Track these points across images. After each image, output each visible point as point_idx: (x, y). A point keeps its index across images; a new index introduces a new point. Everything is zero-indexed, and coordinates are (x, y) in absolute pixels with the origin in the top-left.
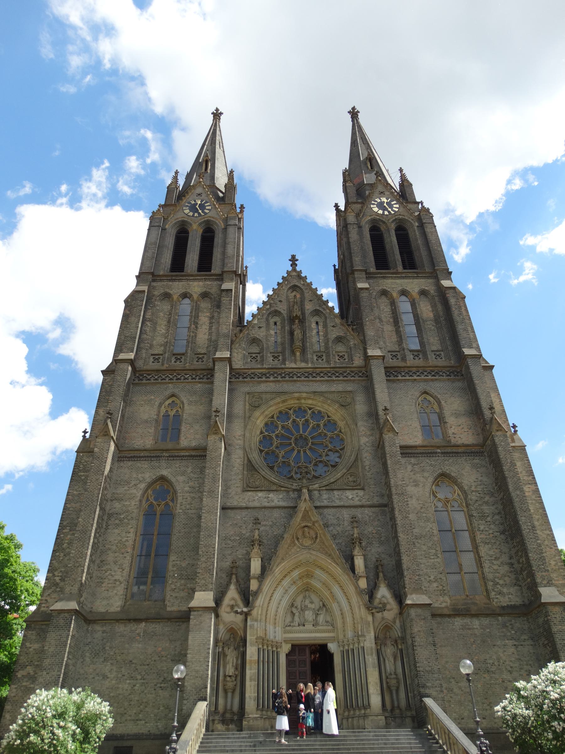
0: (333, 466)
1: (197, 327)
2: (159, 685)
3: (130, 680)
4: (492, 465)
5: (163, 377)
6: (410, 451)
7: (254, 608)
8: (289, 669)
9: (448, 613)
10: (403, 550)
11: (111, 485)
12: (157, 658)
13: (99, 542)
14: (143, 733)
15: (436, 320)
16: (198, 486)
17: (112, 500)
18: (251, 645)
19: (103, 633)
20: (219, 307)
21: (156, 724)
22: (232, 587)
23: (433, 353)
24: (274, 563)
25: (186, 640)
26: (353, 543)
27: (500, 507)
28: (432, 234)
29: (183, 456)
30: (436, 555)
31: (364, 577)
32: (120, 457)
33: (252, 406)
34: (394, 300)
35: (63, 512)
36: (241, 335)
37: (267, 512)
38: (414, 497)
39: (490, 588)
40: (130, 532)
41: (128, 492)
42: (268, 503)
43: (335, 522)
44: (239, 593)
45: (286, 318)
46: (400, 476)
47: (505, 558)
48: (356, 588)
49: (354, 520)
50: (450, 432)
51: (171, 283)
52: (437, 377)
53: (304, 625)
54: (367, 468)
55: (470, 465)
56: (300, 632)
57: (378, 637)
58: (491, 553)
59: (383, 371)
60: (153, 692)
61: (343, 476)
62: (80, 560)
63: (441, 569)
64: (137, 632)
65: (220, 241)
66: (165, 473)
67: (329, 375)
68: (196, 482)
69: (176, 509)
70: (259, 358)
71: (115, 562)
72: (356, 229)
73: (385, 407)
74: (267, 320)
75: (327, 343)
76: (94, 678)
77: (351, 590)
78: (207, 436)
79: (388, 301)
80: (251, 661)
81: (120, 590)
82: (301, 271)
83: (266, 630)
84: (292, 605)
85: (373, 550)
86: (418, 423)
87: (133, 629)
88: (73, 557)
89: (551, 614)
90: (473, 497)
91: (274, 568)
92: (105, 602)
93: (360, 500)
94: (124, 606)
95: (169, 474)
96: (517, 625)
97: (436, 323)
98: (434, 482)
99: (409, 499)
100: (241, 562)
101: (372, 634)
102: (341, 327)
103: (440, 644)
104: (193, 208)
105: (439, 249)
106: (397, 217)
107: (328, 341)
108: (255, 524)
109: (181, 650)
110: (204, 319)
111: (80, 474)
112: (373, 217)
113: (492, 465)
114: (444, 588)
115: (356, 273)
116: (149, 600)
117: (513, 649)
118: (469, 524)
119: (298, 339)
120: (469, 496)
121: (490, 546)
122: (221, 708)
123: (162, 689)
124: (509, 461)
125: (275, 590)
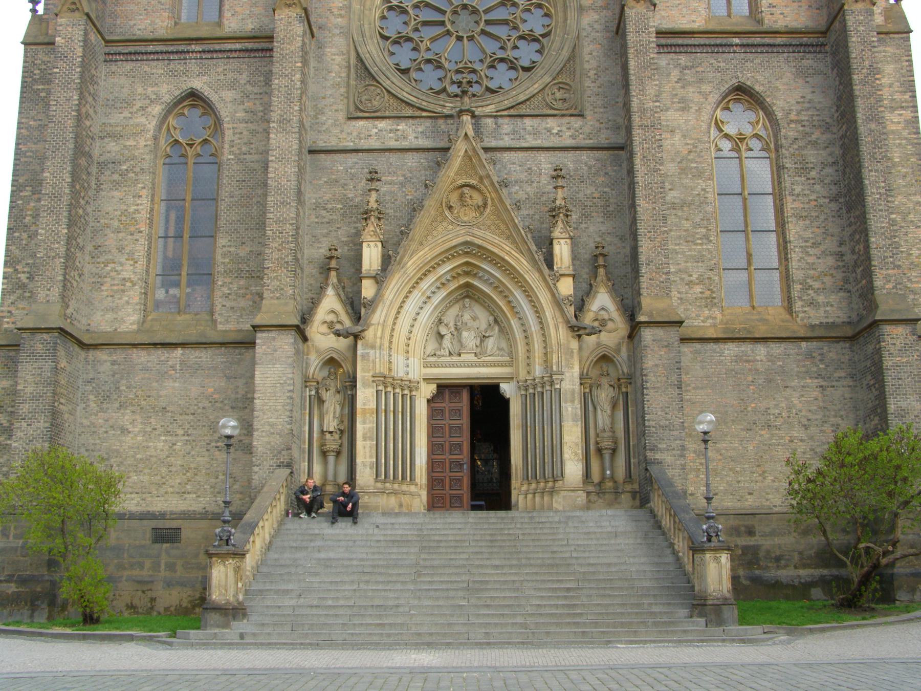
0: (526, 69)
2: (213, 444)
3: (165, 435)
6: (680, 41)
9: (715, 336)
10: (642, 229)
11: (98, 109)
12: (208, 405)
13: (88, 214)
14: (194, 511)
16: (261, 109)
17: (102, 138)
18: (365, 385)
21: (214, 499)
22: (330, 291)
24: (405, 251)
26: (554, 216)
27: (838, 151)
29: (231, 51)
30: (706, 237)
32: (109, 54)
35: (15, 159)
37: (394, 158)
39: (795, 294)
41: (131, 122)
42: (397, 140)
43: (523, 176)
46: (651, 91)
47: (830, 244)
48: (553, 295)
49: (558, 174)
53: (460, 355)
55: (794, 69)
56: (453, 365)
57: (587, 374)
58: (808, 234)
60: (207, 453)
61: (543, 89)
62: (56, 246)
66: (197, 84)
68: (257, 102)
69: (222, 154)
71: (120, 250)
76: (106, 432)
77: (544, 298)
78: (274, 10)
80: (364, 411)
81: (135, 295)
84: (440, 322)
85: (592, 229)
87: (163, 358)
88: (44, 241)
90: (789, 132)
91: (405, 259)
92: (109, 316)
94: (144, 322)
96: (831, 354)
98: (720, 102)
99: (668, 135)
101: (576, 370)
108: (372, 180)
109: (246, 392)
111: (35, 87)
113: (835, 70)
114: (714, 295)
116: (185, 313)
117: (816, 393)
118: (776, 183)
120: (783, 131)
121: (808, 222)
123: (220, 450)
124: (867, 63)
125: (407, 297)
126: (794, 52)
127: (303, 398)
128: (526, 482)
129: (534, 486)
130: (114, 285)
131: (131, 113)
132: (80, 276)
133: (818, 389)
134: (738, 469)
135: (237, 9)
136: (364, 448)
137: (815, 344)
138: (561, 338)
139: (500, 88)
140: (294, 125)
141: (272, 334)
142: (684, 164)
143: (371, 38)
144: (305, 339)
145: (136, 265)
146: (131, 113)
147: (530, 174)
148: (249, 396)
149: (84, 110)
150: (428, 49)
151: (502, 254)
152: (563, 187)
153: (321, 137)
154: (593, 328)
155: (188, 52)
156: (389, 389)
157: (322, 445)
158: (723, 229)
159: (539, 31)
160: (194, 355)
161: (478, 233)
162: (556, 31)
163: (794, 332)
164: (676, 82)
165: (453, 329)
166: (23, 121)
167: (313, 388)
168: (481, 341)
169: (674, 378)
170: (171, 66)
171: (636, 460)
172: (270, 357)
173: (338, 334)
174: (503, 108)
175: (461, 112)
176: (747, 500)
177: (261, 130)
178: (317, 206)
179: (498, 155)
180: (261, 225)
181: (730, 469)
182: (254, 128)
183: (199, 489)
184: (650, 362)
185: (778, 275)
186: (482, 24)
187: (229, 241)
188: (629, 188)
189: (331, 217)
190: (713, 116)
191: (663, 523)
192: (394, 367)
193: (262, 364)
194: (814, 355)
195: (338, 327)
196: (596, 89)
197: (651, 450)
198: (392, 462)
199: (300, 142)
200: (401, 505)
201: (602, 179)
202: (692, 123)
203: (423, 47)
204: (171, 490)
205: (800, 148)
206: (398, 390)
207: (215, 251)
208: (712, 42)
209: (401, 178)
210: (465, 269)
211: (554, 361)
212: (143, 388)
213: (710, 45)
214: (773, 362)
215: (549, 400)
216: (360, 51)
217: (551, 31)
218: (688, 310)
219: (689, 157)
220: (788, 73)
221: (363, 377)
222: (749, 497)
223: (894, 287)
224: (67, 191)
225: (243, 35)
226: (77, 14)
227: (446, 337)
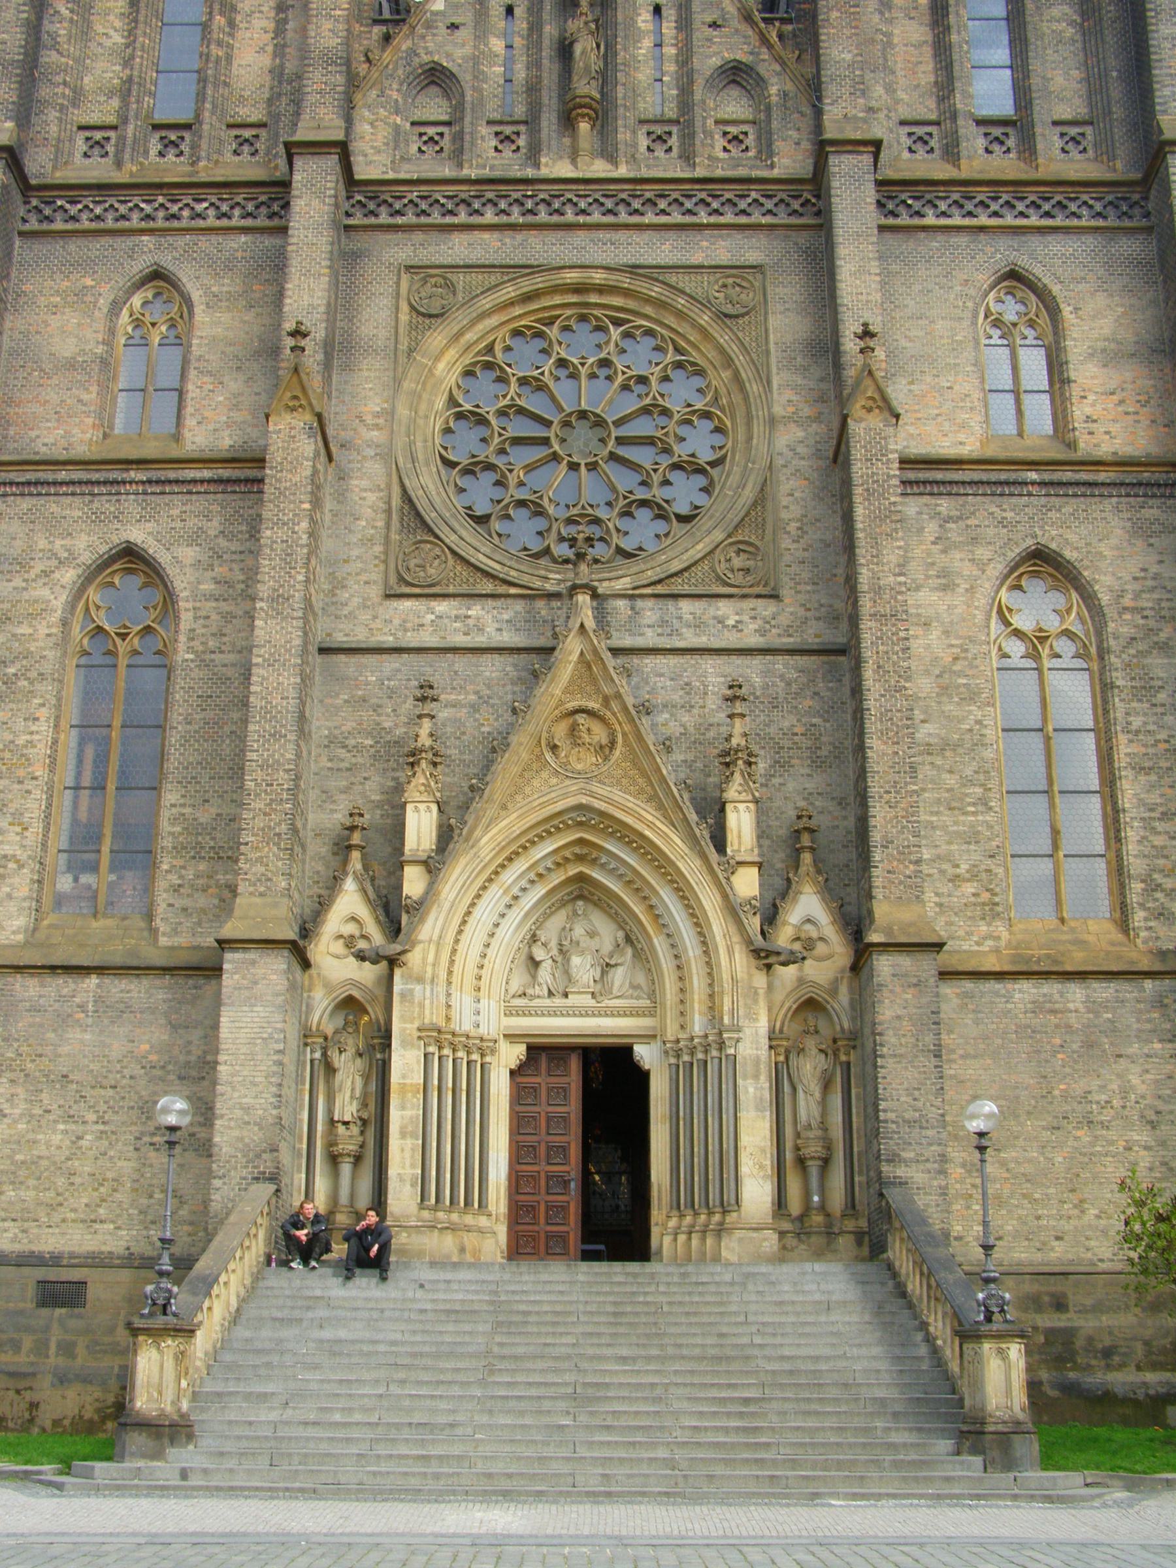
0: (683, 519)
2: (147, 1139)
3: (65, 1122)
5: (123, 209)
6: (939, 476)
7: (413, 946)
8: (518, 1108)
9: (997, 969)
10: (875, 786)
16: (242, 577)
18: (405, 1044)
22: (350, 885)
24: (478, 819)
25: (216, 1026)
26: (727, 765)
29: (194, 481)
31: (752, 864)
33: (419, 313)
36: (387, 56)
37: (460, 663)
40: (37, 719)
43: (677, 697)
46: (891, 557)
48: (725, 896)
49: (734, 694)
50: (1079, 412)
52: (1058, 221)
53: (566, 995)
55: (1129, 524)
58: (1154, 798)
59: (870, 194)
60: (135, 1155)
61: (712, 552)
63: (994, 843)
64: (77, 1000)
66: (137, 535)
67: (688, 204)
68: (234, 566)
70: (446, 143)
73: (865, 325)
77: (710, 900)
78: (267, 416)
80: (403, 1087)
83: (449, 1006)
84: (534, 939)
85: (791, 786)
86: (977, 382)
87: (65, 991)
91: (478, 833)
93: (762, 632)
94: (35, 929)
98: (1007, 577)
99: (920, 631)
101: (763, 1024)
103: (961, 1052)
107: (691, 82)
108: (423, 699)
109: (205, 1052)
114: (997, 899)
116: (105, 916)
118: (1100, 711)
119: (587, 69)
120: (1111, 626)
121: (1153, 778)
125: (478, 896)
126: (1128, 495)
127: (300, 1063)
128: (675, 1213)
129: (688, 1219)
134: (1037, 1196)
135: (206, 414)
139: (640, 549)
140: (296, 606)
141: (252, 955)
143: (428, 465)
144: (306, 964)
145: (27, 834)
148: (209, 1058)
150: (521, 484)
151: (639, 826)
152: (743, 716)
153: (341, 626)
154: (792, 952)
155: (124, 482)
156: (446, 1051)
157: (331, 1144)
158: (1012, 788)
159: (705, 456)
160: (119, 988)
161: (600, 791)
163: (1132, 962)
164: (933, 543)
165: (555, 952)
167: (318, 1047)
169: (929, 1039)
171: (864, 1179)
172: (247, 993)
173: (361, 957)
174: (645, 582)
176: (1052, 1249)
178: (331, 741)
179: (636, 660)
180: (237, 771)
181: (1024, 1196)
182: (228, 609)
183: (118, 1216)
185: (1104, 866)
186: (611, 443)
187: (183, 796)
188: (855, 719)
189: (354, 760)
190: (994, 600)
191: (910, 1287)
193: (232, 1004)
194: (1166, 1001)
195: (362, 945)
196: (800, 554)
197: (888, 1161)
198: (448, 1176)
199: (306, 634)
200: (462, 1250)
201: (808, 702)
202: (959, 610)
203: (512, 480)
205: (1141, 654)
206: (460, 1054)
207: (157, 814)
208: (993, 477)
209: (473, 697)
210: (577, 850)
211: (726, 1008)
212: (31, 1041)
213: (988, 483)
214: (1097, 1014)
216: (407, 482)
218: (951, 924)
221: (405, 1029)
222: (1057, 1243)
227: (544, 964)
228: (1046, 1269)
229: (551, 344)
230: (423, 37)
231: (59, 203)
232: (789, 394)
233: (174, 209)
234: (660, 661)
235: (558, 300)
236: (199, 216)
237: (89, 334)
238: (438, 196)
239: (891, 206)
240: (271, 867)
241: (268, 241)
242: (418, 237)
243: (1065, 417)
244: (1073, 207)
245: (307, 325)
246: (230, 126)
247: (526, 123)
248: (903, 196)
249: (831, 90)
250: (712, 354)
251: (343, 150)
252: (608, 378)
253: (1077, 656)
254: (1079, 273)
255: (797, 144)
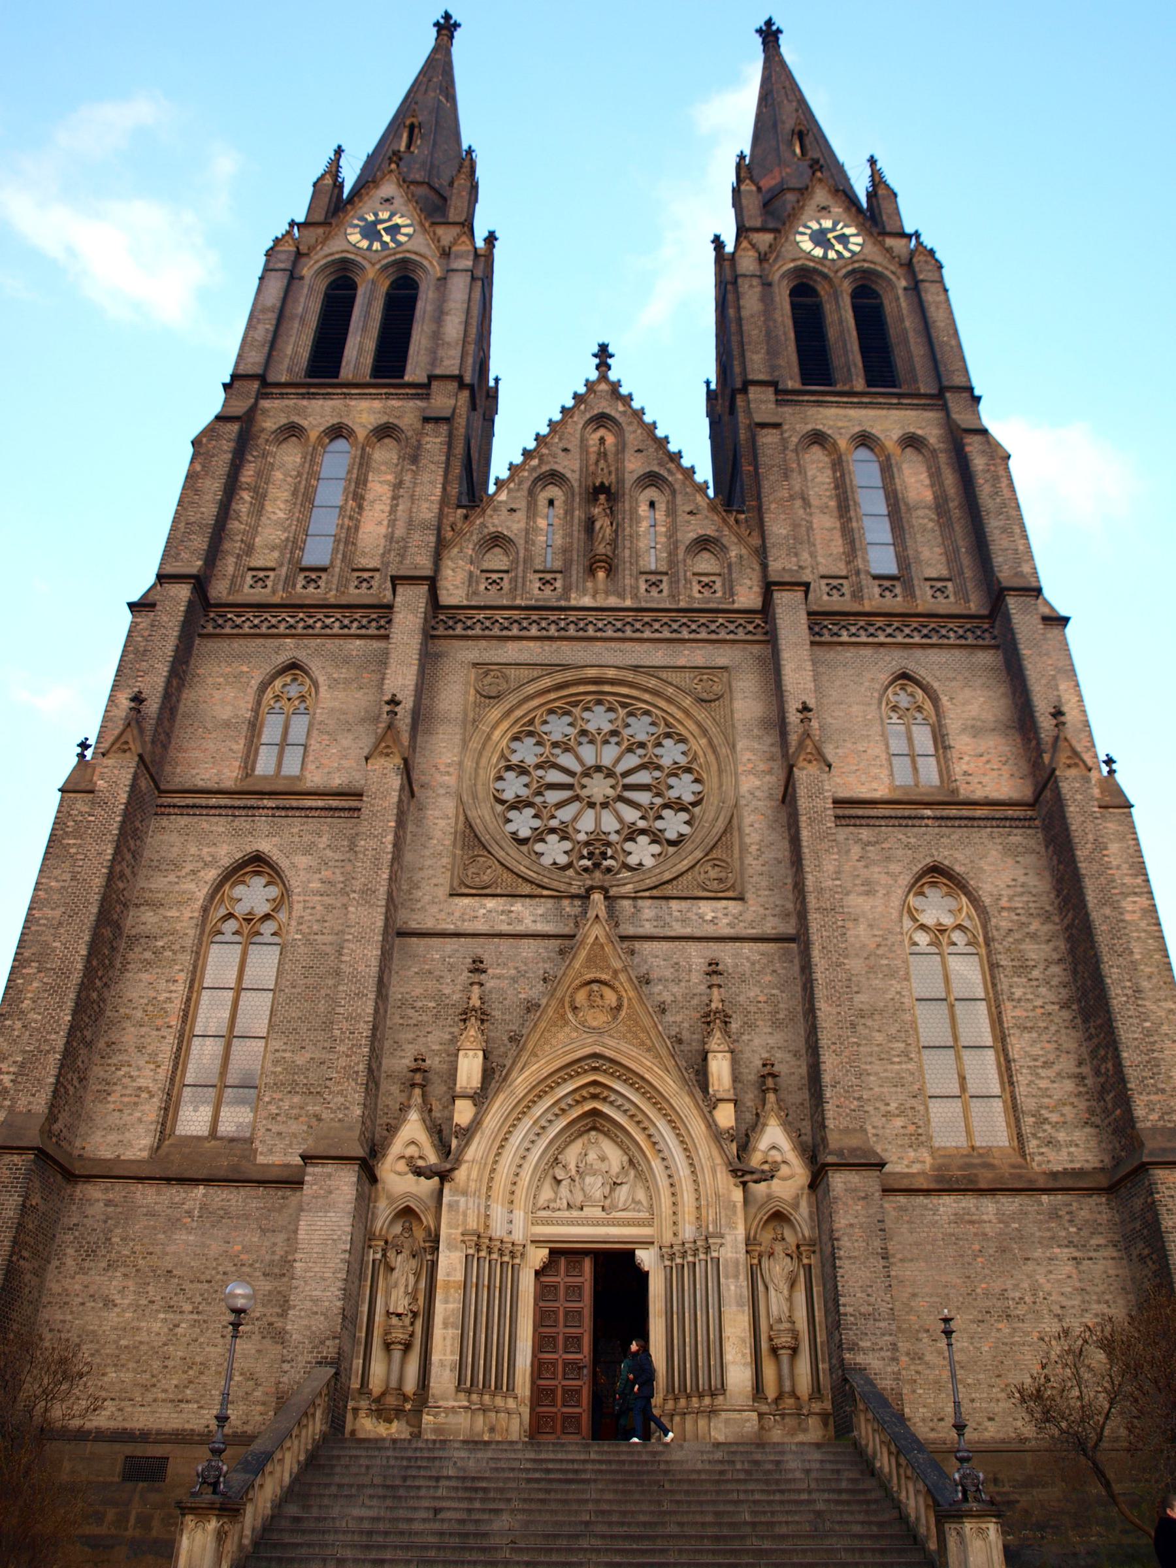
0: (671, 843)
1: (360, 507)
4: (1051, 848)
5: (274, 621)
6: (860, 812)
7: (460, 1165)
8: (541, 1304)
9: (925, 1186)
10: (825, 1039)
15: (940, 506)
16: (342, 879)
18: (451, 1247)
19: (106, 1205)
20: (415, 459)
22: (414, 1116)
23: (929, 583)
26: (708, 1023)
28: (938, 308)
29: (311, 809)
30: (905, 1054)
33: (481, 695)
34: (840, 457)
37: (504, 945)
38: (861, 920)
39: (1027, 1130)
41: (177, 888)
42: (509, 924)
43: (668, 973)
44: (428, 1129)
45: (577, 490)
46: (829, 866)
47: (1067, 1064)
48: (709, 1126)
49: (714, 969)
50: (958, 768)
51: (305, 402)
52: (934, 640)
54: (753, 848)
55: (1000, 847)
58: (1036, 1050)
62: (53, 1036)
63: (916, 1087)
65: (429, 308)
66: (265, 846)
67: (675, 626)
68: (337, 871)
71: (140, 1049)
72: (758, 289)
73: (804, 703)
74: (531, 492)
75: (672, 553)
77: (697, 1128)
79: (826, 459)
80: (447, 1283)
82: (619, 381)
85: (757, 1042)
88: (38, 1030)
89: (1162, 1188)
90: (1002, 921)
91: (514, 1074)
92: (113, 1138)
94: (158, 1148)
95: (275, 850)
96: (1082, 1213)
97: (938, 514)
98: (913, 885)
99: (849, 924)
100: (437, 1059)
101: (741, 1231)
102: (710, 515)
103: (899, 1256)
104: (370, 232)
105: (953, 342)
106: (856, 265)
107: (676, 548)
109: (286, 1252)
110: (379, 488)
111: (65, 841)
112: (799, 263)
114: (920, 1131)
115: (752, 389)
117: (1069, 1268)
120: (994, 921)
121: (1034, 1035)
122: (376, 1383)
126: (998, 827)
130: (125, 1095)
131: (178, 877)
132: (81, 1080)
133: (1070, 1263)
134: (970, 1381)
136: (444, 1339)
137: (1060, 1198)
138: (720, 1186)
140: (381, 897)
141: (329, 1169)
142: (872, 960)
144: (373, 1179)
145: (159, 1070)
146: (178, 877)
147: (677, 971)
148: (290, 1258)
149: (118, 868)
152: (720, 986)
154: (763, 1172)
155: (259, 808)
159: (688, 798)
160: (220, 1196)
161: (610, 1043)
162: (708, 799)
163: (1030, 1181)
165: (573, 1172)
166: (43, 881)
167: (379, 1249)
168: (612, 1190)
169: (877, 1243)
170: (235, 824)
171: (827, 1366)
172: (321, 1201)
173: (418, 1172)
175: (590, 890)
176: (986, 1429)
177: (339, 905)
178: (403, 1004)
179: (637, 945)
182: (330, 902)
183: (202, 1396)
184: (842, 1221)
185: (1001, 1104)
187: (285, 1044)
192: (493, 1224)
194: (1060, 1213)
195: (420, 1163)
196: (759, 868)
197: (850, 1350)
198: (482, 1362)
199: (387, 919)
200: (492, 1430)
201: (768, 978)
202: (879, 909)
204: (164, 1396)
208: (899, 813)
209: (513, 972)
210: (592, 1090)
212: (146, 1240)
213: (896, 818)
214: (1007, 1224)
215: (703, 1274)
216: (469, 813)
217: (702, 799)
219: (879, 952)
220: (994, 853)
221: (450, 1235)
222: (990, 1423)
223: (1161, 1118)
224: (80, 966)
225: (327, 790)
226: (128, 754)
228: (983, 1447)
229: (575, 719)
230: (491, 516)
231: (229, 616)
232: (748, 755)
233: (311, 621)
234: (655, 945)
235: (582, 689)
236: (327, 626)
237: (242, 705)
238: (498, 617)
239: (817, 629)
240: (349, 1098)
241: (376, 645)
242: (483, 643)
243: (948, 772)
244: (944, 632)
245: (399, 697)
246: (354, 570)
247: (561, 572)
248: (826, 623)
249: (773, 553)
250: (693, 727)
251: (432, 583)
252: (617, 744)
253: (969, 944)
254: (951, 675)
255: (750, 588)
